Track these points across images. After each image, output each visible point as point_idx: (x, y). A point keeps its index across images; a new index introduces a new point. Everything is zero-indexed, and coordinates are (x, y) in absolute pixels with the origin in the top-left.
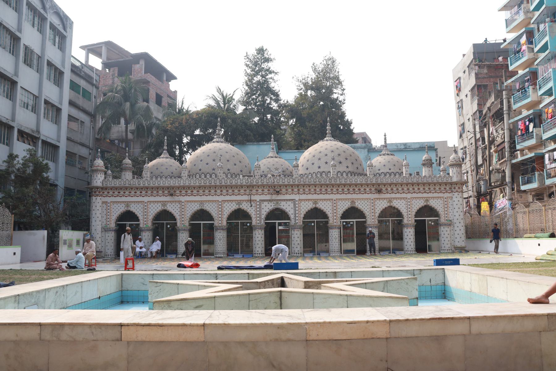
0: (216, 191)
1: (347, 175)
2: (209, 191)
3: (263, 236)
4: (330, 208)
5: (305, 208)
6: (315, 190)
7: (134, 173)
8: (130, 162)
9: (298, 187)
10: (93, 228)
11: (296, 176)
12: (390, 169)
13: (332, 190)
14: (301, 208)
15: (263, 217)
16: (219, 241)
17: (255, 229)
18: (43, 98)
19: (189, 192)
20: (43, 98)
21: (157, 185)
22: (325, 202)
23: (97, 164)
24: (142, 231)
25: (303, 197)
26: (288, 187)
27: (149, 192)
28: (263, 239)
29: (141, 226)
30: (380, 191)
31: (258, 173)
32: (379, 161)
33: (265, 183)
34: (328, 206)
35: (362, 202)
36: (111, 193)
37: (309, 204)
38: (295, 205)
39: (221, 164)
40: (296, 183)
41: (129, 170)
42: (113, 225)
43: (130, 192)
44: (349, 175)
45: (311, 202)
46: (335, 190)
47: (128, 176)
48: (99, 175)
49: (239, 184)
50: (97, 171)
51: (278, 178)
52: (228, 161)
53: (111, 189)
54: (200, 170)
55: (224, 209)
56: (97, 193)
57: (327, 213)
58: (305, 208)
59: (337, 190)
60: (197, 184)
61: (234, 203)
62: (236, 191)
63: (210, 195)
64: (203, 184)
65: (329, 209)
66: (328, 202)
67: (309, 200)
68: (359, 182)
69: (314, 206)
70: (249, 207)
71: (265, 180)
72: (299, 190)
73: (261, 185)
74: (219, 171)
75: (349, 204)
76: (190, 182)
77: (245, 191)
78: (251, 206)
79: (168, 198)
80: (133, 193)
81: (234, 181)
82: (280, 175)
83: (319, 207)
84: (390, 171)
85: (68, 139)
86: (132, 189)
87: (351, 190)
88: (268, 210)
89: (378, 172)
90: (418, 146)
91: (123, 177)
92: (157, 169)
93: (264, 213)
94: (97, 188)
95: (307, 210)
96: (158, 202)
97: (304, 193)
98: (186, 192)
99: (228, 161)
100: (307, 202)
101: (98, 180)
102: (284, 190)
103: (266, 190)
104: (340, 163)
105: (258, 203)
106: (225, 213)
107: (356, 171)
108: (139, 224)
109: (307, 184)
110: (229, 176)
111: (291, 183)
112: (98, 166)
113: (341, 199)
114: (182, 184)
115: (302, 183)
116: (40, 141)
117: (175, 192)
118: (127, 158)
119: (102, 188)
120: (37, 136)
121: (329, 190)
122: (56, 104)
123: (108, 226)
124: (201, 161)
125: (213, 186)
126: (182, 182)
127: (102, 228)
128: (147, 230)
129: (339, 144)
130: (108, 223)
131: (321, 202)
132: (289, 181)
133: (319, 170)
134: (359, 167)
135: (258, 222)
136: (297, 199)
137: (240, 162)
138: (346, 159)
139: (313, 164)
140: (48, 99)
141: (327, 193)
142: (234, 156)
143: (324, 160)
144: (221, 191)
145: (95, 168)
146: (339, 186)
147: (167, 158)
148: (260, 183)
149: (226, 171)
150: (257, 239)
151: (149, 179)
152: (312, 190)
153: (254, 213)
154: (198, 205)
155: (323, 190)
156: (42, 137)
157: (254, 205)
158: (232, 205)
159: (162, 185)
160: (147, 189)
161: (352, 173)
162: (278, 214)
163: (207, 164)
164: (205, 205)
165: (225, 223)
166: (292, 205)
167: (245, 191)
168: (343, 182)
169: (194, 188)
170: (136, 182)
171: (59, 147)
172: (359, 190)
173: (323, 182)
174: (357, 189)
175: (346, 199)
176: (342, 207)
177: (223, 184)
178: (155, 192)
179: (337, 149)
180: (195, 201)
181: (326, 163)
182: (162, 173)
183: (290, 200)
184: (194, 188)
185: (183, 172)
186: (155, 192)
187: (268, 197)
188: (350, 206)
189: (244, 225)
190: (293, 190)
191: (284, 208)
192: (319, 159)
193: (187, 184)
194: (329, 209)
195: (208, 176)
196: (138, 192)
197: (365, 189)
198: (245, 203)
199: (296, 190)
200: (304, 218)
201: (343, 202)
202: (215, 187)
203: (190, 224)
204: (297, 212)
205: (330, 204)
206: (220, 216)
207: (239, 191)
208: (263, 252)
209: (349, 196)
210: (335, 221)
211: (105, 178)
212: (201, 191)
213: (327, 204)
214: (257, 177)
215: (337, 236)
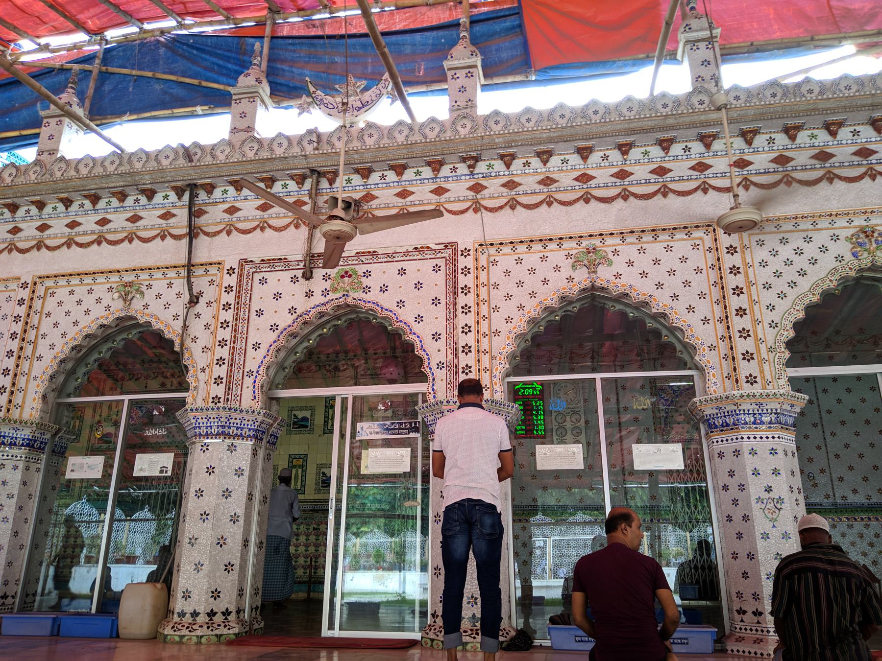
4: (701, 283)
5: (520, 296)
14: (497, 297)
15: (254, 360)
22: (656, 249)
34: (685, 272)
37: (545, 270)
45: (556, 256)
55: (46, 326)
57: (679, 316)
58: (520, 296)
61: (101, 290)
65: (688, 297)
67: (545, 241)
69: (582, 278)
70: (179, 307)
75: (844, 248)
77: (167, 216)
78: (194, 300)
83: (616, 287)
88: (285, 320)
93: (263, 338)
95: (533, 308)
100: (532, 259)
106: (43, 348)
135: (220, 390)
136: (466, 241)
144: (43, 228)
153: (205, 338)
166: (437, 284)
176: (790, 274)
188: (851, 267)
189: (151, 422)
191: (387, 301)
194: (688, 297)
198: (160, 285)
204: (462, 320)
205: (699, 259)
210: (745, 368)
213: (670, 261)
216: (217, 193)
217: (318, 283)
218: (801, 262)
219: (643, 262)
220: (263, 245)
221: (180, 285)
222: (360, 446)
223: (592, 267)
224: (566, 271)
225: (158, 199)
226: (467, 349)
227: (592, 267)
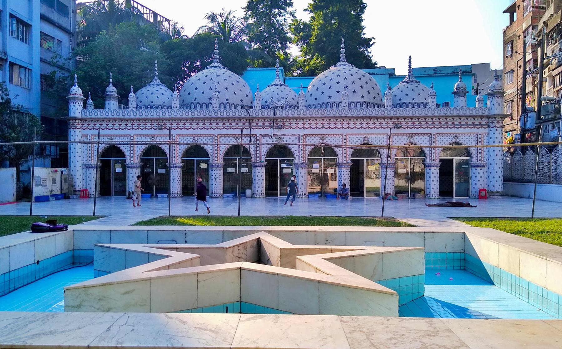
0: (211, 124)
1: (362, 106)
2: (204, 124)
3: (264, 175)
6: (323, 124)
7: (120, 102)
8: (115, 89)
9: (303, 120)
10: (72, 165)
11: (302, 107)
12: (413, 99)
13: (342, 124)
15: (264, 153)
16: (214, 180)
17: (255, 167)
18: (8, 12)
19: (181, 124)
20: (8, 12)
21: (144, 116)
22: (333, 137)
23: (74, 92)
24: (129, 167)
25: (309, 131)
26: (291, 120)
27: (136, 125)
28: (264, 177)
29: (127, 162)
30: (397, 126)
31: (258, 104)
32: (401, 90)
33: (266, 116)
35: (377, 137)
36: (92, 125)
38: (299, 140)
39: (217, 94)
40: (302, 115)
41: (113, 98)
42: (94, 161)
43: (114, 125)
44: (364, 106)
45: (317, 137)
46: (345, 123)
47: (112, 104)
48: (77, 105)
49: (237, 116)
50: (74, 99)
51: (281, 109)
52: (227, 89)
53: (92, 121)
54: (195, 99)
56: (76, 125)
59: (348, 124)
60: (190, 116)
61: (231, 138)
62: (234, 124)
63: (204, 128)
64: (196, 116)
66: (338, 137)
68: (374, 115)
69: (321, 141)
71: (266, 113)
72: (304, 124)
73: (261, 118)
74: (215, 101)
75: (362, 139)
76: (181, 114)
79: (157, 132)
80: (117, 125)
81: (231, 113)
82: (283, 107)
84: (413, 101)
85: (42, 60)
86: (116, 121)
87: (364, 123)
89: (400, 102)
90: (450, 71)
91: (107, 106)
92: (147, 97)
93: (265, 149)
94: (75, 119)
96: (146, 135)
97: (310, 128)
98: (178, 124)
99: (227, 89)
100: (313, 138)
101: (76, 110)
102: (287, 124)
103: (267, 124)
104: (354, 92)
105: (258, 138)
107: (372, 101)
108: (125, 160)
109: (314, 117)
110: (228, 107)
111: (296, 115)
112: (76, 94)
113: (353, 134)
114: (173, 116)
115: (308, 115)
116: (8, 64)
117: (165, 124)
118: (111, 85)
119: (81, 119)
120: (3, 57)
121: (339, 124)
122: (25, 20)
123: (90, 163)
124: (196, 89)
125: (207, 118)
126: (173, 113)
127: (83, 164)
128: (134, 167)
129: (356, 69)
130: (90, 159)
131: (329, 137)
132: (293, 113)
133: (330, 100)
134: (377, 97)
135: (258, 159)
137: (240, 91)
138: (362, 87)
139: (323, 93)
140: (14, 14)
141: (336, 128)
142: (233, 84)
143: (334, 89)
144: (217, 124)
145: (72, 96)
146: (350, 120)
147: (158, 85)
148: (260, 116)
149: (225, 101)
150: (257, 178)
151: (134, 109)
152: (320, 124)
153: (253, 148)
154: (192, 140)
155: (332, 123)
156: (10, 59)
157: (253, 140)
158: (229, 140)
159: (149, 116)
160: (133, 120)
161: (367, 104)
162: (281, 150)
163: (203, 93)
164: (199, 140)
165: (221, 160)
167: (244, 124)
168: (355, 115)
169: (187, 120)
170: (120, 113)
171: (31, 70)
172: (374, 123)
173: (331, 115)
174: (371, 123)
175: (358, 134)
177: (219, 116)
178: (142, 125)
179: (352, 75)
180: (188, 135)
181: (338, 92)
182: (152, 102)
183: (294, 135)
184: (187, 120)
185: (173, 102)
186: (142, 125)
187: (269, 132)
190: (297, 124)
192: (330, 87)
193: (178, 116)
195: (204, 107)
196: (123, 125)
197: (381, 123)
199: (301, 123)
200: (309, 155)
201: (355, 137)
202: (210, 119)
203: (183, 161)
206: (216, 152)
207: (237, 124)
208: (264, 192)
209: (362, 131)
210: (344, 159)
211: (85, 107)
212: (194, 124)
214: (257, 109)
215: (346, 177)
216: (254, 121)
217: (274, 140)
218: (355, 141)
219: (331, 140)
220: (264, 132)
221: (248, 138)
222: (282, 169)
223: (323, 140)
224: (319, 140)
225: (242, 121)
226: (302, 154)
227: (323, 140)
